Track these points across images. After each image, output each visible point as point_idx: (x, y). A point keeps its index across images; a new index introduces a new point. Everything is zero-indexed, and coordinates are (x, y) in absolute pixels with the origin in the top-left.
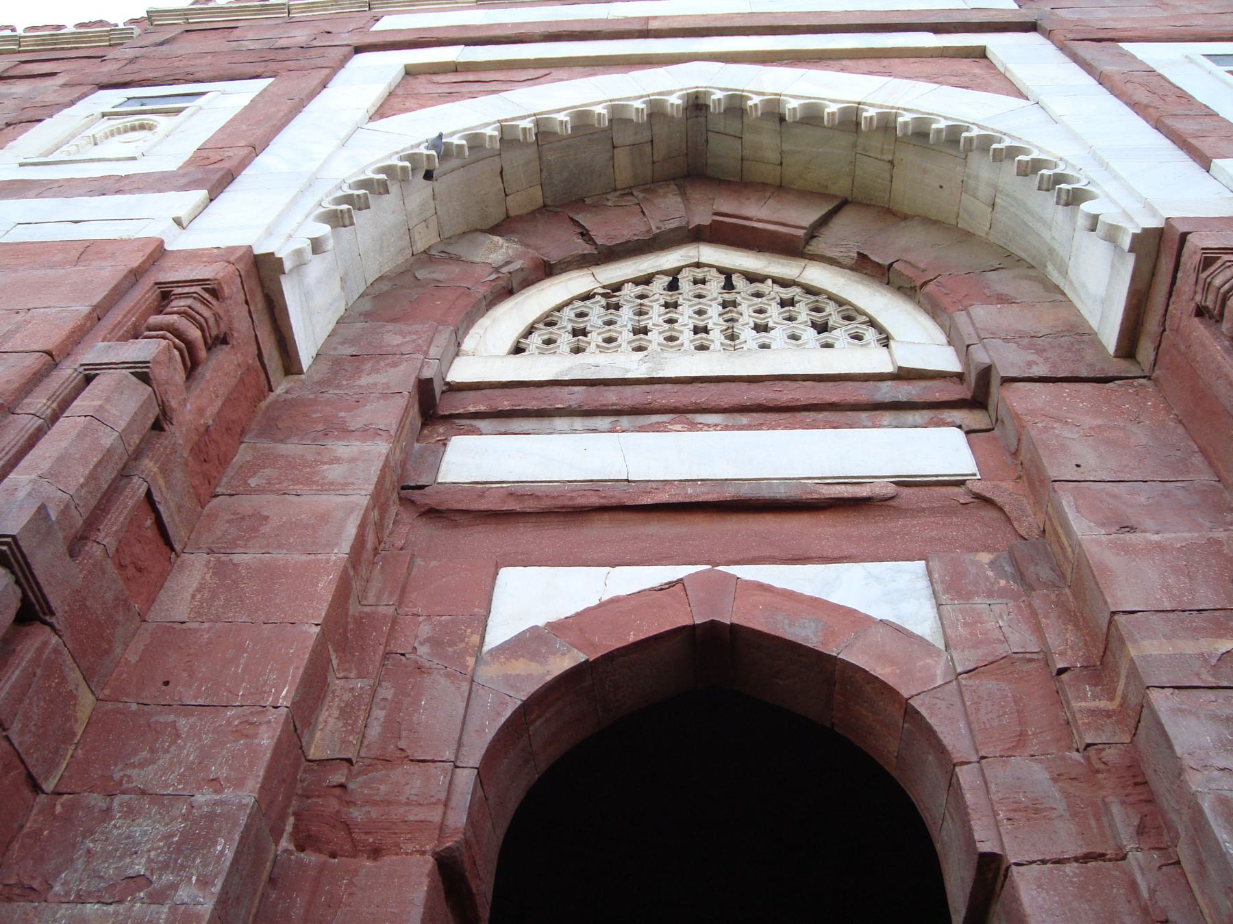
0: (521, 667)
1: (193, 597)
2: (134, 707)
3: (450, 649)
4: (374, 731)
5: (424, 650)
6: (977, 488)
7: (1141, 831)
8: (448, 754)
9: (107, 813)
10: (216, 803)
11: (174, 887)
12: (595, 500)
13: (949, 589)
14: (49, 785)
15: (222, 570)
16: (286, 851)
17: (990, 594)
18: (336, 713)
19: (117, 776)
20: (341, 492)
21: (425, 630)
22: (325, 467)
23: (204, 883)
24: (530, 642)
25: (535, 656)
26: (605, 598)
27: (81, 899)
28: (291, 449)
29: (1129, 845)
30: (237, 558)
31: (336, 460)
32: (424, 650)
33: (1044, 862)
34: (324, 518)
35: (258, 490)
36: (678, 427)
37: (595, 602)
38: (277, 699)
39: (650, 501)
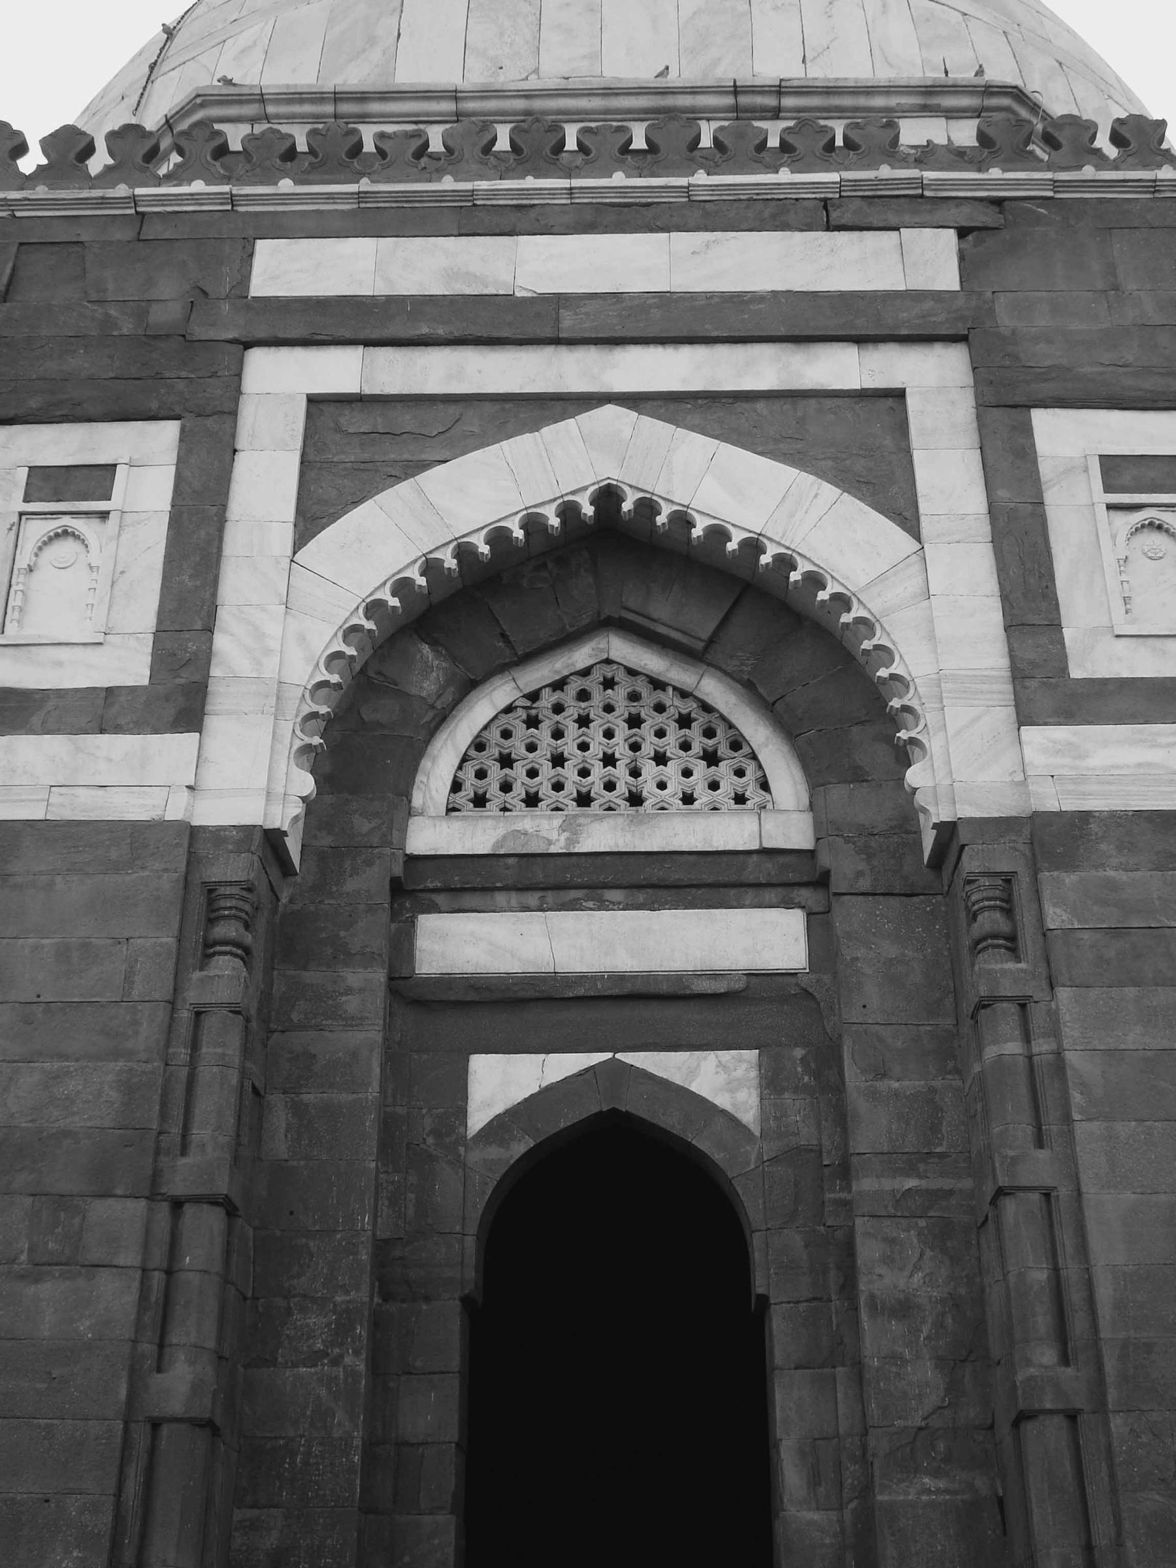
0: (494, 1152)
1: (286, 1136)
2: (278, 1233)
3: (448, 1140)
4: (411, 1212)
5: (430, 1140)
6: (804, 981)
7: (843, 1287)
8: (458, 1228)
9: (289, 1311)
10: (349, 1302)
11: (341, 1356)
12: (531, 993)
13: (772, 1082)
14: (250, 1294)
15: (298, 1110)
16: (378, 1304)
17: (796, 1090)
18: (386, 1203)
19: (286, 1285)
20: (360, 1028)
21: (428, 1123)
22: (344, 999)
23: (357, 1353)
24: (499, 1127)
25: (503, 1143)
26: (544, 1085)
27: (295, 1365)
28: (312, 977)
29: (834, 1297)
30: (306, 1098)
31: (349, 991)
32: (430, 1140)
33: (789, 1302)
34: (355, 1055)
35: (302, 1027)
36: (590, 904)
37: (537, 1089)
38: (363, 1225)
39: (571, 995)
